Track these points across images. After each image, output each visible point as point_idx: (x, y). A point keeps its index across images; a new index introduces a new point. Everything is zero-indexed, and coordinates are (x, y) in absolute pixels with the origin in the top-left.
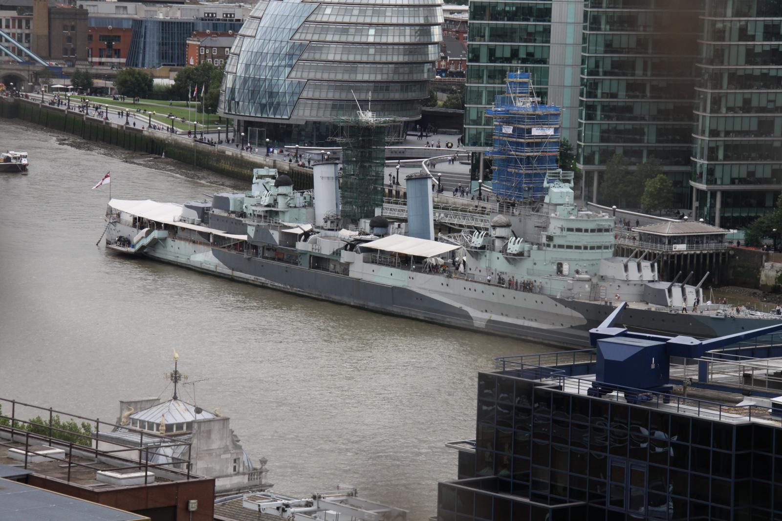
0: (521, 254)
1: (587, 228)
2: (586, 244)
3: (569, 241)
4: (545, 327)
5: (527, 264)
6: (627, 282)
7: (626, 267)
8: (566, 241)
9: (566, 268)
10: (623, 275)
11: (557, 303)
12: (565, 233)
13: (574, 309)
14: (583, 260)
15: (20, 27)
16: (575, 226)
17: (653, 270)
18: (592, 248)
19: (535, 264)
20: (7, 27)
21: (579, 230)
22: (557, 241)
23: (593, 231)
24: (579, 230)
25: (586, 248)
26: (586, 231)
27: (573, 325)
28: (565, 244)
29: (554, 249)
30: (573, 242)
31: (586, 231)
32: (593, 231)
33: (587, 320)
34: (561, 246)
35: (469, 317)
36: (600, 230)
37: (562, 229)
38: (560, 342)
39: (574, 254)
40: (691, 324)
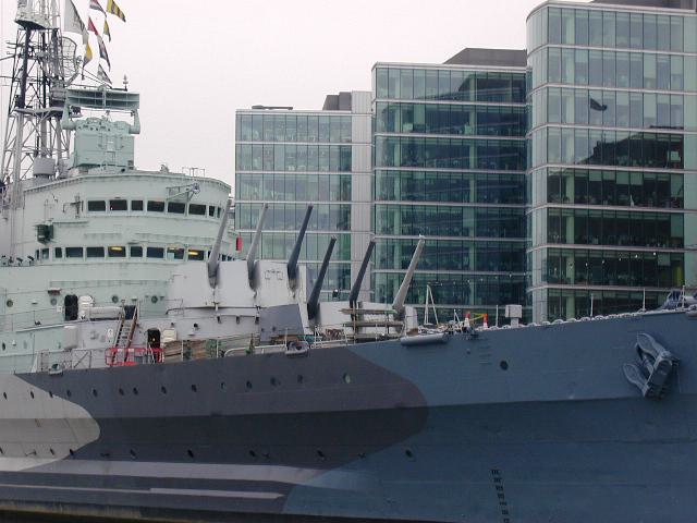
1: (137, 198)
2: (137, 239)
3: (94, 235)
7: (214, 274)
8: (86, 236)
9: (84, 303)
10: (204, 296)
11: (36, 390)
12: (85, 213)
13: (69, 395)
14: (128, 283)
16: (106, 193)
17: (294, 287)
19: (9, 303)
21: (119, 205)
22: (63, 239)
23: (155, 207)
24: (119, 205)
25: (136, 252)
26: (137, 206)
27: (75, 448)
28: (85, 244)
29: (59, 261)
30: (103, 235)
31: (137, 206)
32: (155, 207)
33: (101, 422)
34: (74, 252)
36: (176, 208)
37: (77, 204)
38: (46, 503)
40: (348, 380)
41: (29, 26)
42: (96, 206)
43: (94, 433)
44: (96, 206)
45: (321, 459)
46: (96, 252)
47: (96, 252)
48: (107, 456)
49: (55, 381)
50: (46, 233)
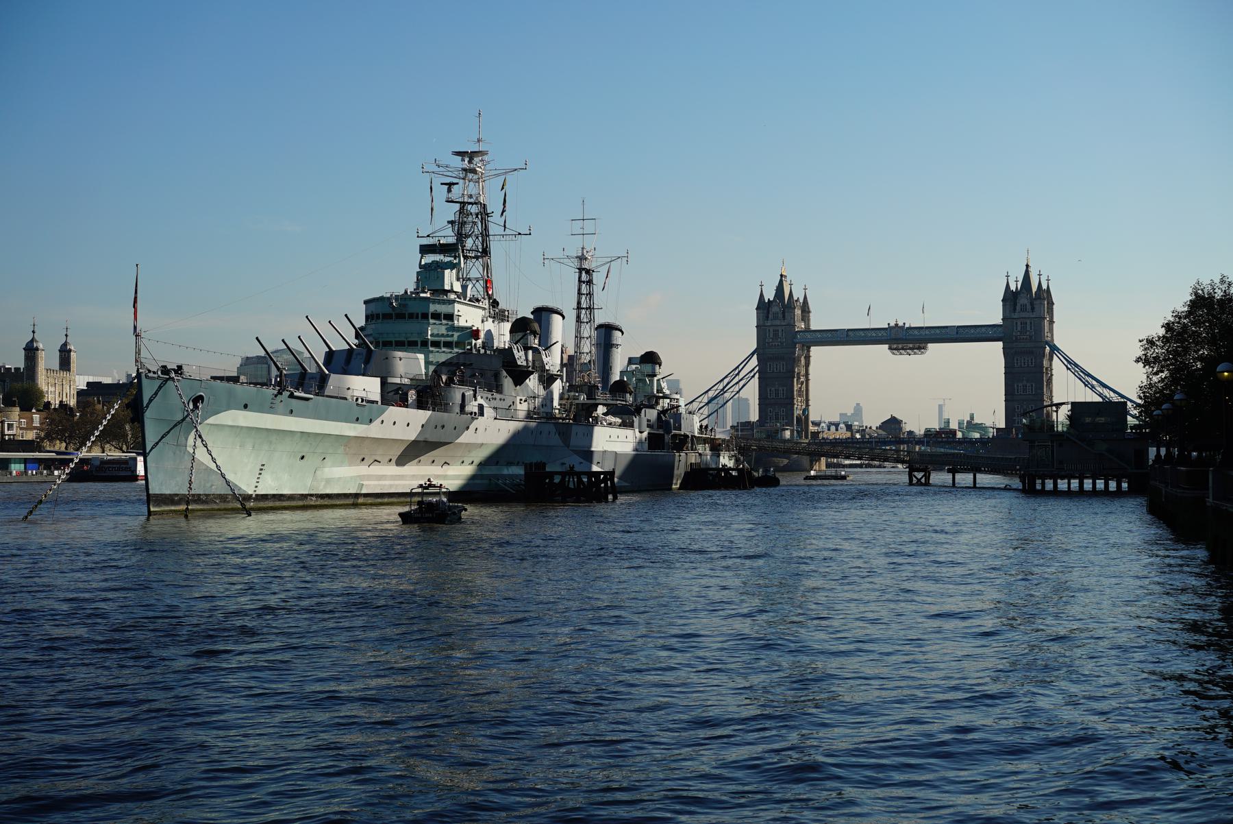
23: (387, 316)
32: (387, 316)
41: (463, 204)
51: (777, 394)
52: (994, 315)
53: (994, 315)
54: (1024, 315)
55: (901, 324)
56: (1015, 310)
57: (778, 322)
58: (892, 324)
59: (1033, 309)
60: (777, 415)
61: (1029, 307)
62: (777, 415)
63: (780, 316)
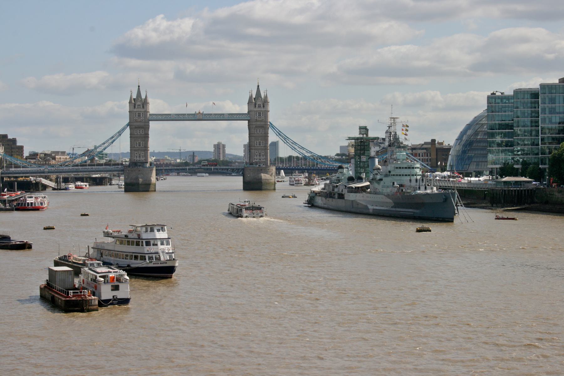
0: (381, 180)
4: (386, 208)
5: (382, 182)
6: (410, 187)
7: (410, 180)
9: (396, 185)
15: (427, 156)
16: (398, 166)
18: (406, 175)
20: (422, 156)
21: (400, 168)
22: (392, 173)
23: (406, 168)
24: (400, 168)
32: (406, 168)
34: (394, 175)
35: (369, 209)
36: (409, 168)
39: (398, 178)
42: (397, 168)
43: (393, 204)
44: (397, 168)
45: (417, 209)
46: (397, 175)
47: (397, 175)
48: (395, 207)
49: (388, 196)
50: (390, 172)
51: (139, 145)
52: (245, 109)
53: (245, 109)
54: (259, 109)
55: (201, 112)
56: (255, 106)
57: (139, 110)
58: (197, 112)
59: (264, 106)
60: (140, 155)
61: (262, 106)
62: (140, 155)
63: (141, 106)
